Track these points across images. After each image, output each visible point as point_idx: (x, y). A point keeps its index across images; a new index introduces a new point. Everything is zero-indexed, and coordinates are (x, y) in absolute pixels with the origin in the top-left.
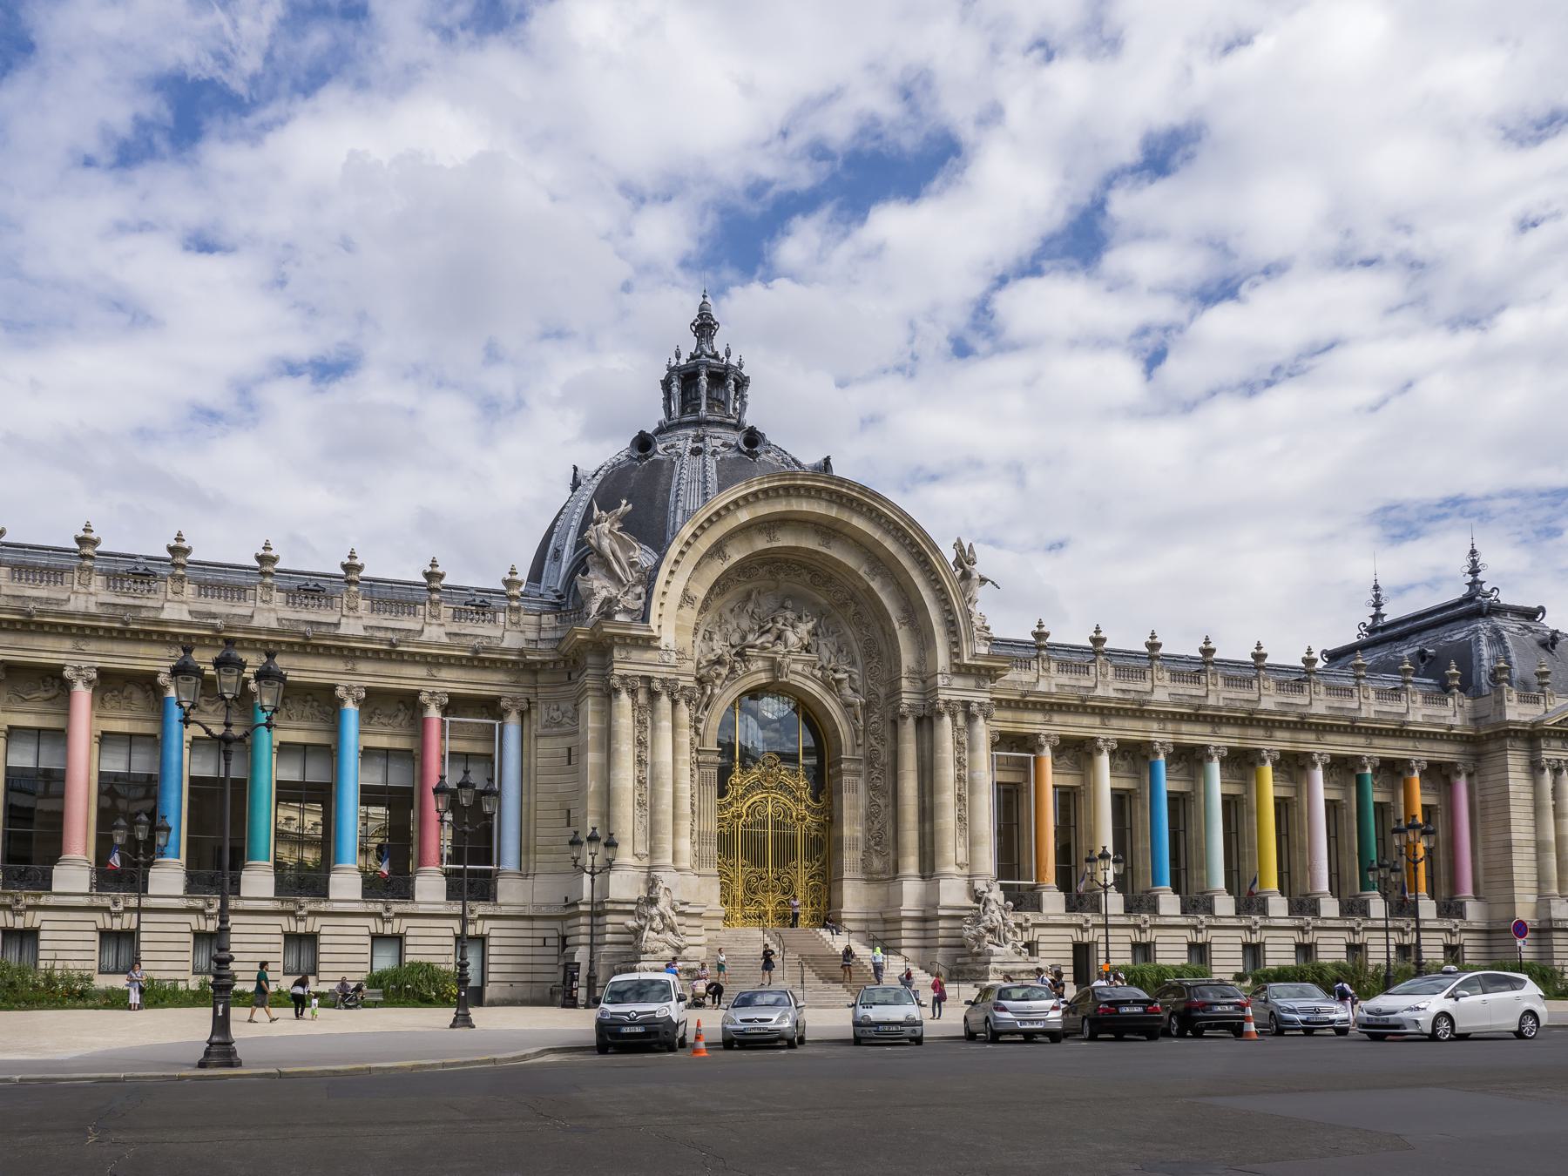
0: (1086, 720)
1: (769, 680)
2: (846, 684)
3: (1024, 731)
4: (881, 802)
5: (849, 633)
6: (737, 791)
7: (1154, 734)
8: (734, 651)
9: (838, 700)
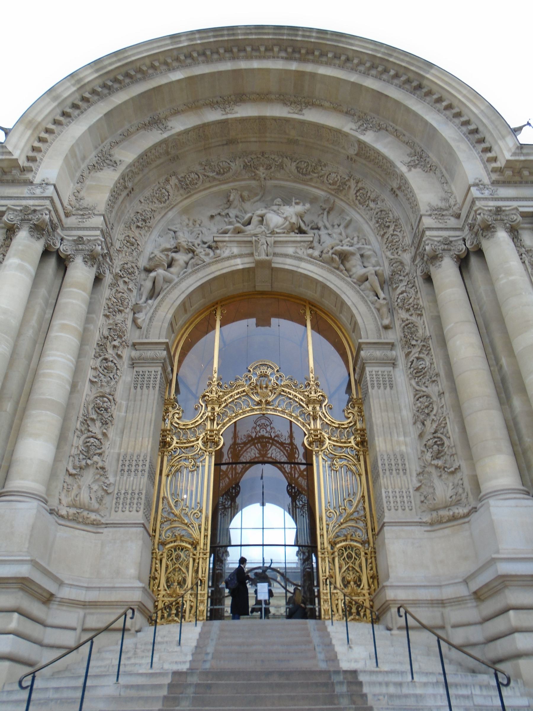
1: (247, 266)
2: (355, 262)
4: (432, 390)
5: (357, 217)
6: (213, 409)
8: (206, 245)
9: (349, 279)
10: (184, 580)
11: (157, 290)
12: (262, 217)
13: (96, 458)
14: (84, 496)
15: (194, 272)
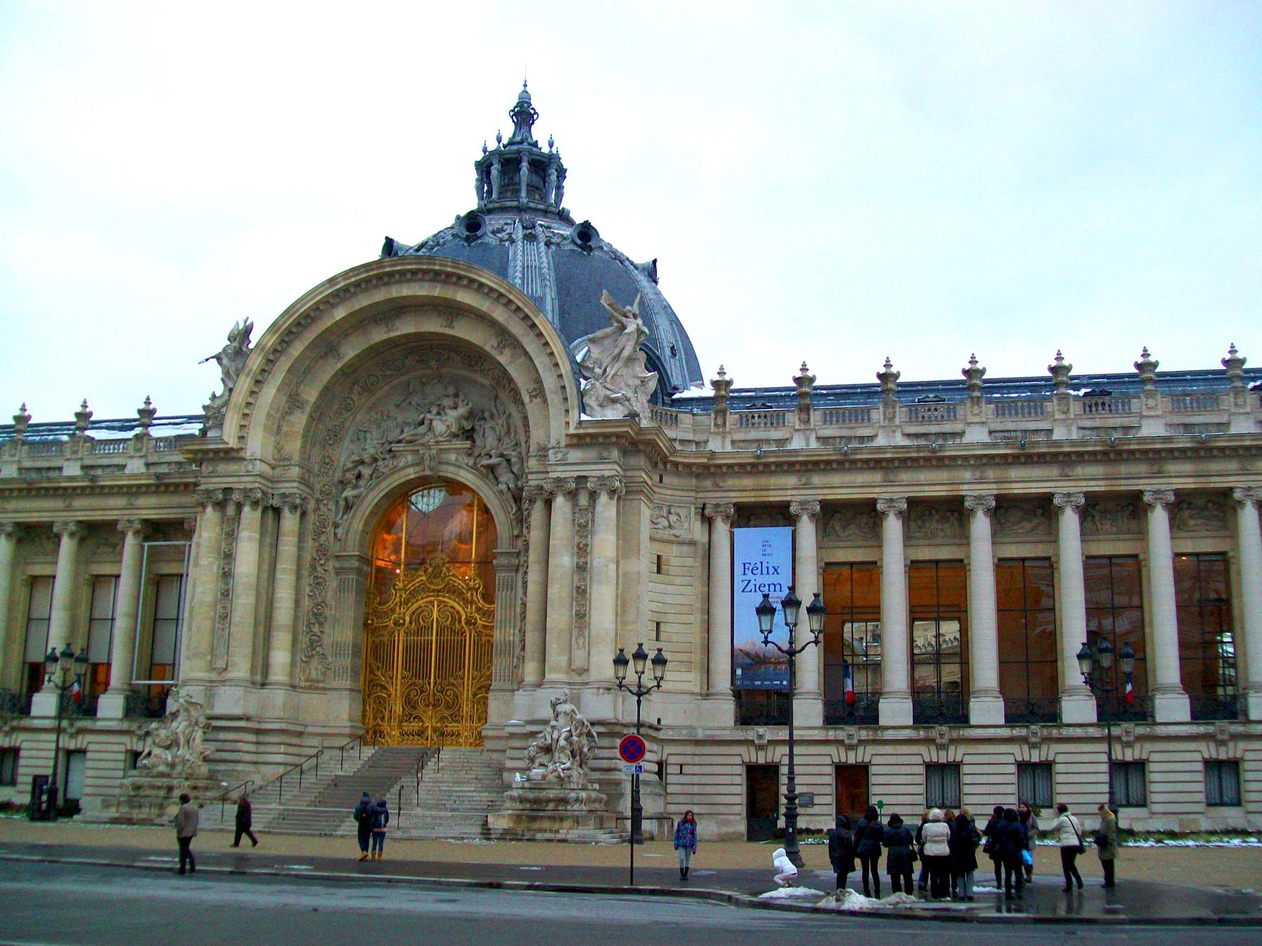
0: (860, 478)
1: (418, 475)
3: (771, 499)
7: (966, 487)
9: (495, 488)
10: (384, 717)
11: (350, 504)
12: (431, 420)
13: (318, 649)
14: (314, 675)
15: (377, 484)
